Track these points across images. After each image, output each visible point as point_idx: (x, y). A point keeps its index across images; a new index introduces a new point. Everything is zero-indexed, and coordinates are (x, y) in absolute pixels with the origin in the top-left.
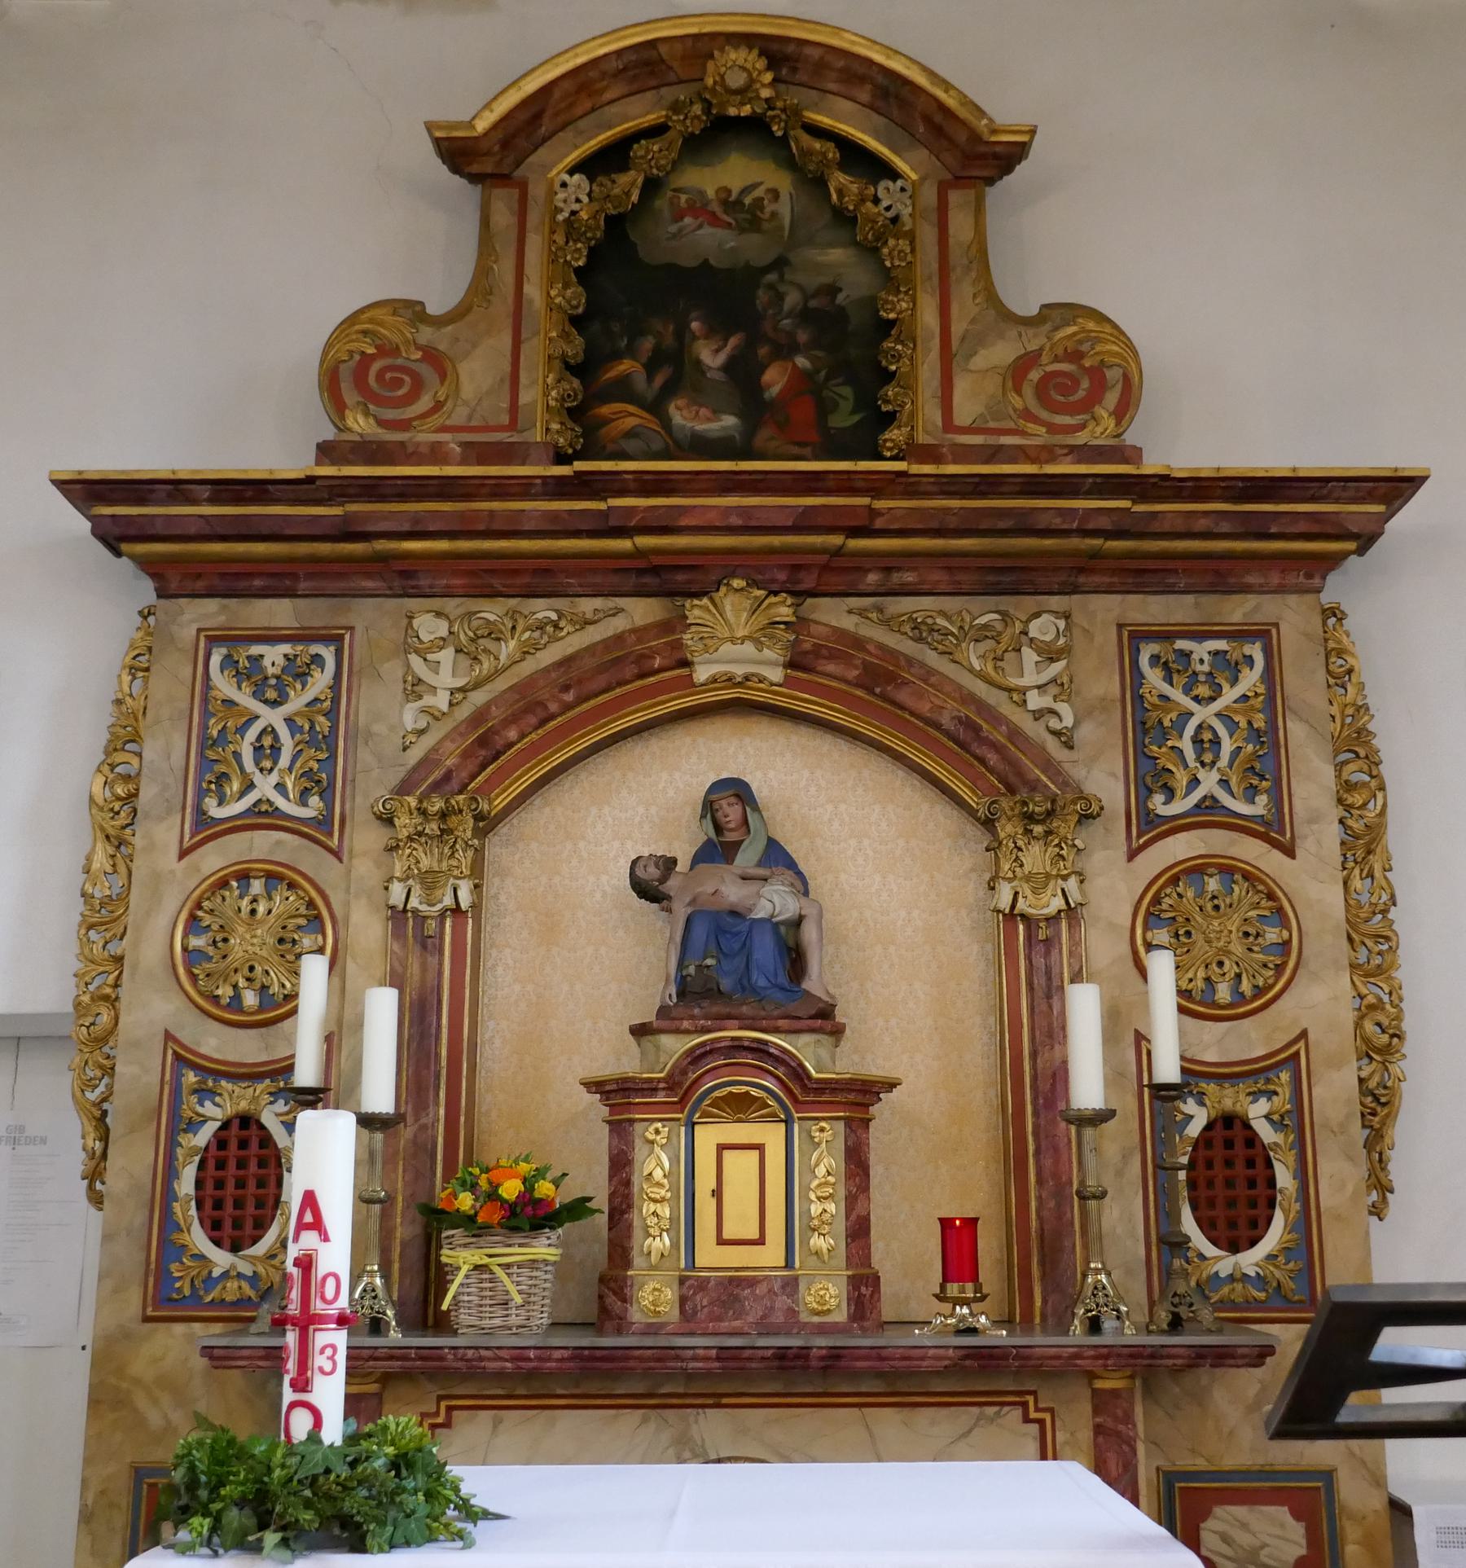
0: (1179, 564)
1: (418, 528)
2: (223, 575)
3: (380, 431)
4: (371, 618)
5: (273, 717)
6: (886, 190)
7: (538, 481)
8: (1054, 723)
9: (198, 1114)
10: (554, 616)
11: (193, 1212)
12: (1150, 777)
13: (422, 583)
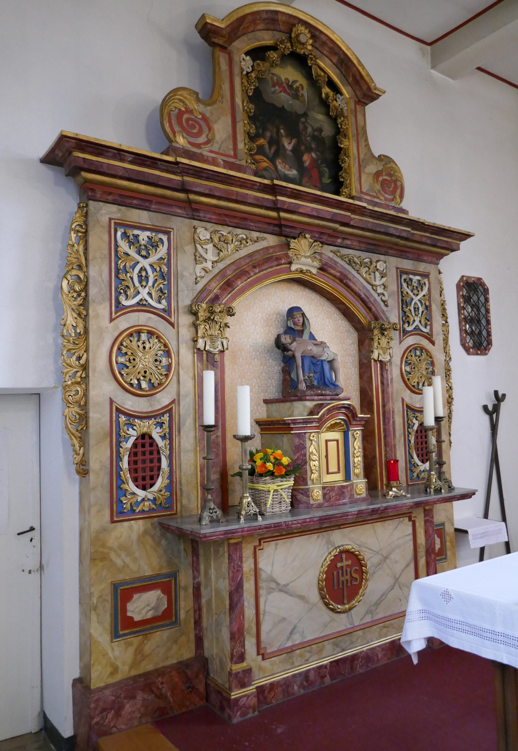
0: (411, 250)
1: (211, 193)
2: (120, 195)
3: (190, 146)
4: (180, 225)
7: (258, 184)
8: (383, 298)
9: (127, 434)
10: (245, 237)
11: (129, 475)
12: (405, 319)
13: (201, 215)
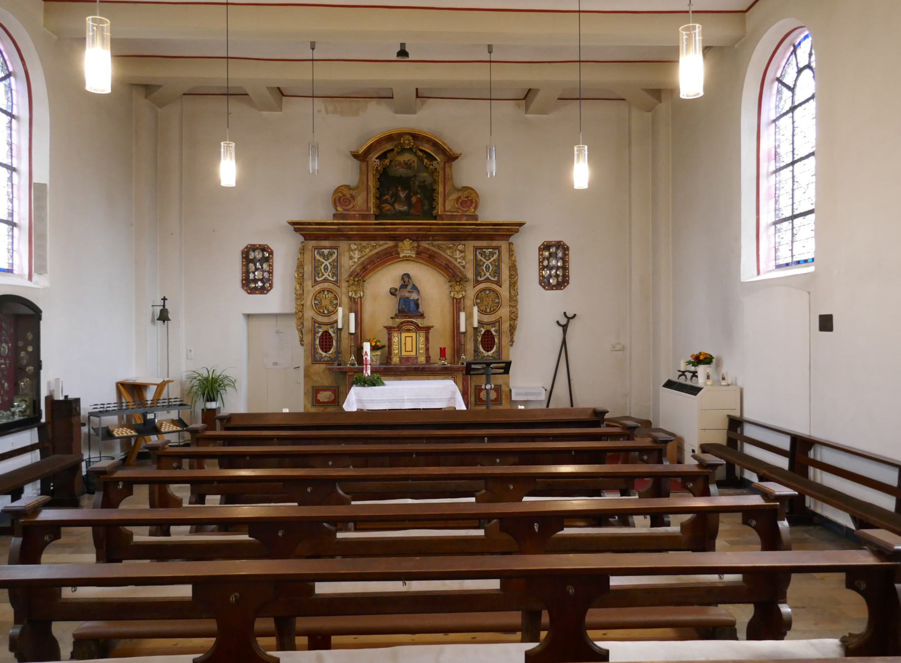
4: (343, 245)
5: (327, 263)
6: (434, 163)
12: (477, 273)
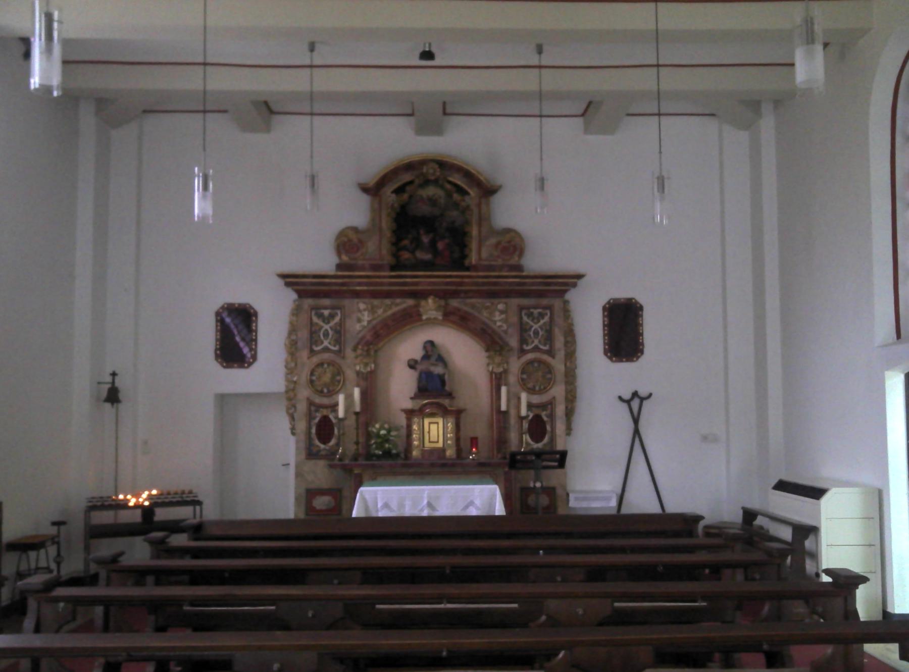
5: (327, 327)
6: (467, 198)
12: (523, 341)
